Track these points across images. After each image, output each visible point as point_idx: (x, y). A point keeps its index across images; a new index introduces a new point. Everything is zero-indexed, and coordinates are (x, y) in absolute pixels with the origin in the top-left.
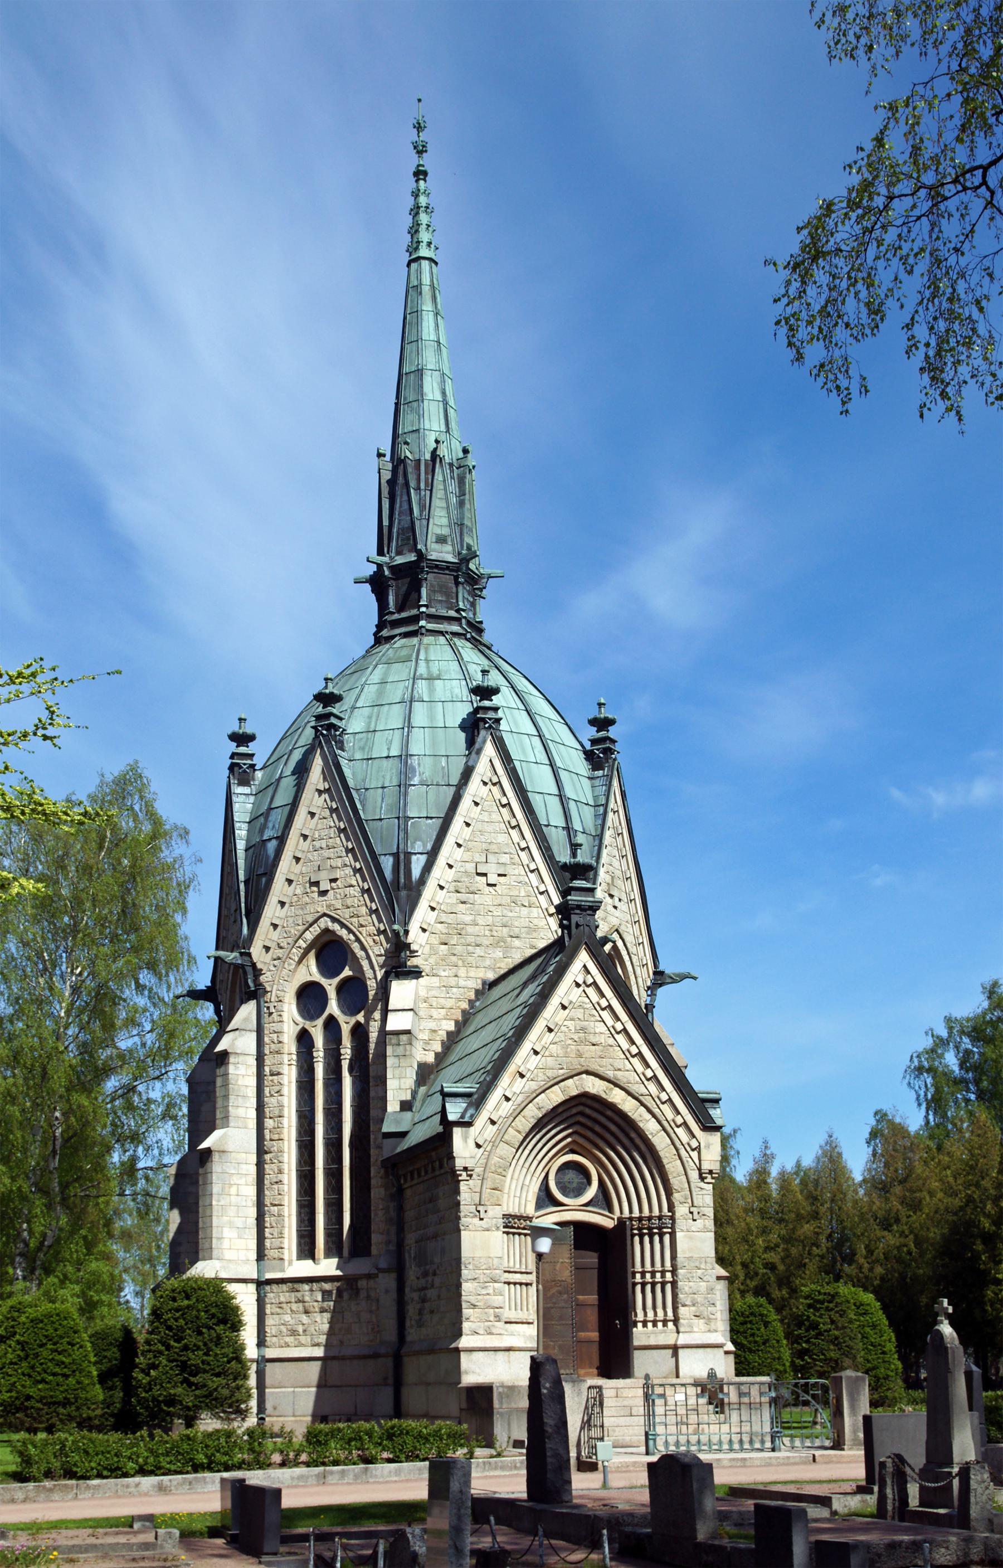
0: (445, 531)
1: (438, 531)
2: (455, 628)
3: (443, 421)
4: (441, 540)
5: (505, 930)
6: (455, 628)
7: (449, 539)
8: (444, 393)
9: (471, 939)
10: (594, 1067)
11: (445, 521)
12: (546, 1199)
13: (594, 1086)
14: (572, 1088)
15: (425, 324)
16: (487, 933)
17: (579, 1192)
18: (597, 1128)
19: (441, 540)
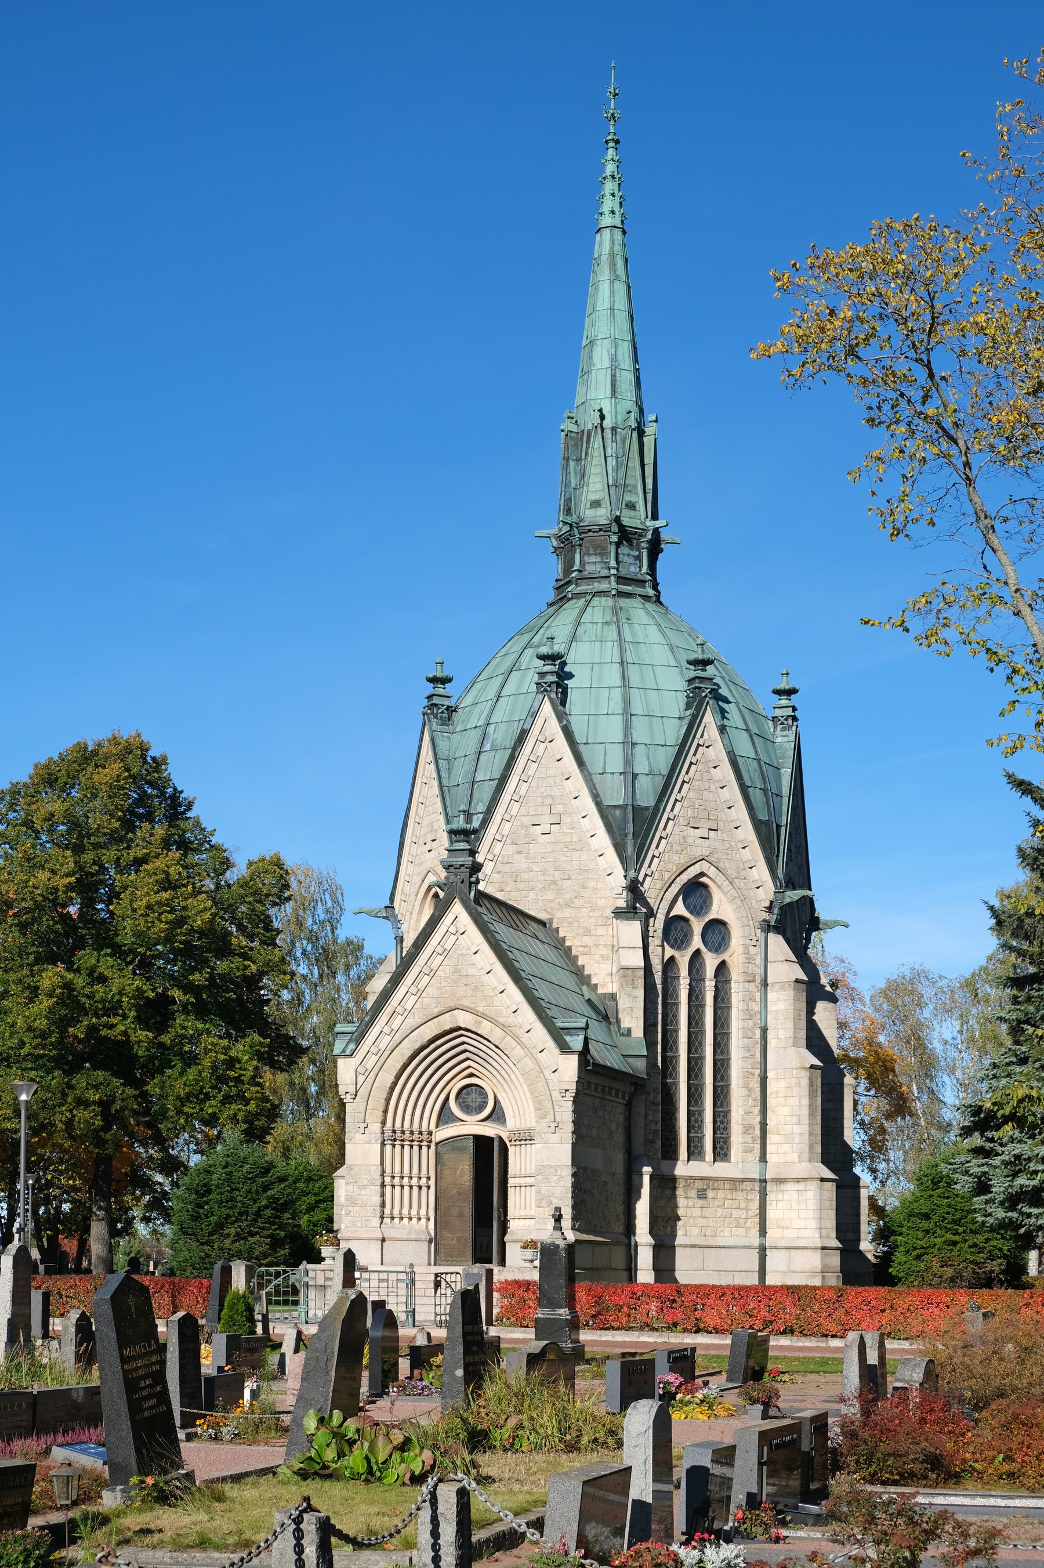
0: (598, 496)
1: (592, 497)
2: (604, 586)
3: (609, 387)
4: (596, 504)
5: (557, 873)
6: (604, 586)
7: (603, 503)
8: (614, 359)
9: (522, 885)
10: (466, 1003)
11: (599, 486)
12: (444, 1116)
13: (463, 1019)
14: (446, 1022)
15: (600, 294)
16: (541, 878)
17: (481, 1108)
18: (481, 1054)
19: (596, 504)
